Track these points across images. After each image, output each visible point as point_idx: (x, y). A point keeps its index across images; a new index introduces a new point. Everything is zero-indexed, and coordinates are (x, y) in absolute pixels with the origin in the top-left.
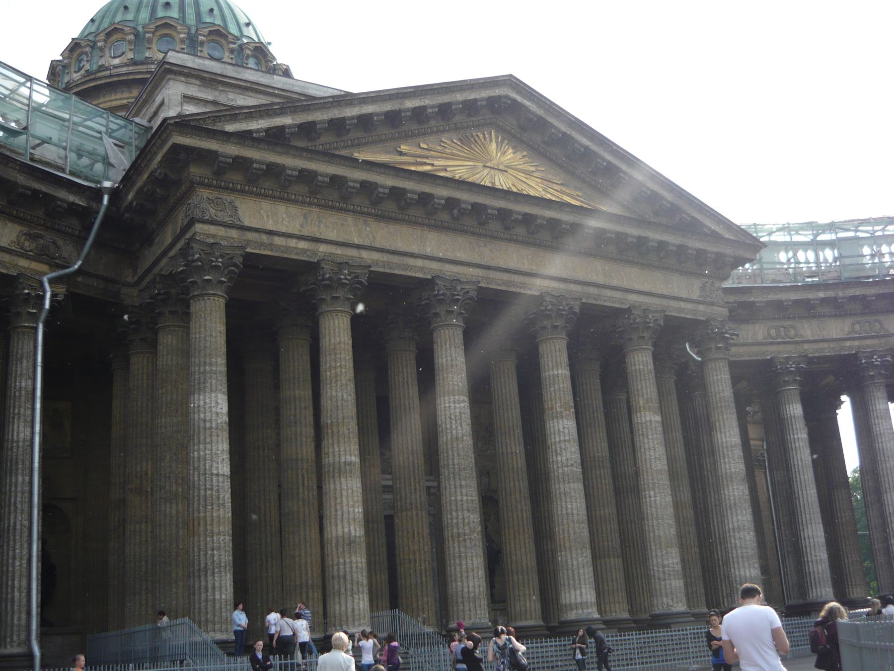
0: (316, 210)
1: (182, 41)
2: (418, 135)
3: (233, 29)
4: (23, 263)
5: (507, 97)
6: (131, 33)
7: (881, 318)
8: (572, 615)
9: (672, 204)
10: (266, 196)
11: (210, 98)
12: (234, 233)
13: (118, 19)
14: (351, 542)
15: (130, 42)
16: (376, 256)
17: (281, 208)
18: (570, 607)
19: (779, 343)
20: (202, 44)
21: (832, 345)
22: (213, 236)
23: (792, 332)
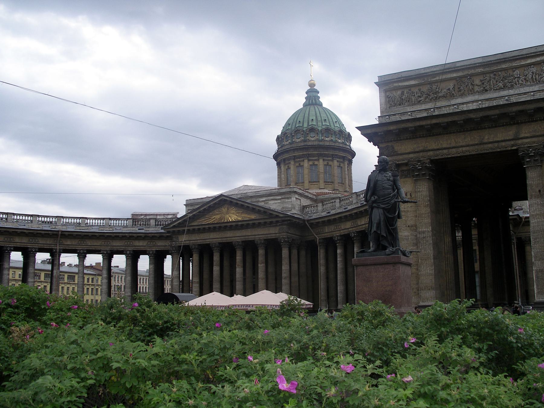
2: (209, 212)
5: (223, 199)
16: (200, 241)
20: (294, 136)
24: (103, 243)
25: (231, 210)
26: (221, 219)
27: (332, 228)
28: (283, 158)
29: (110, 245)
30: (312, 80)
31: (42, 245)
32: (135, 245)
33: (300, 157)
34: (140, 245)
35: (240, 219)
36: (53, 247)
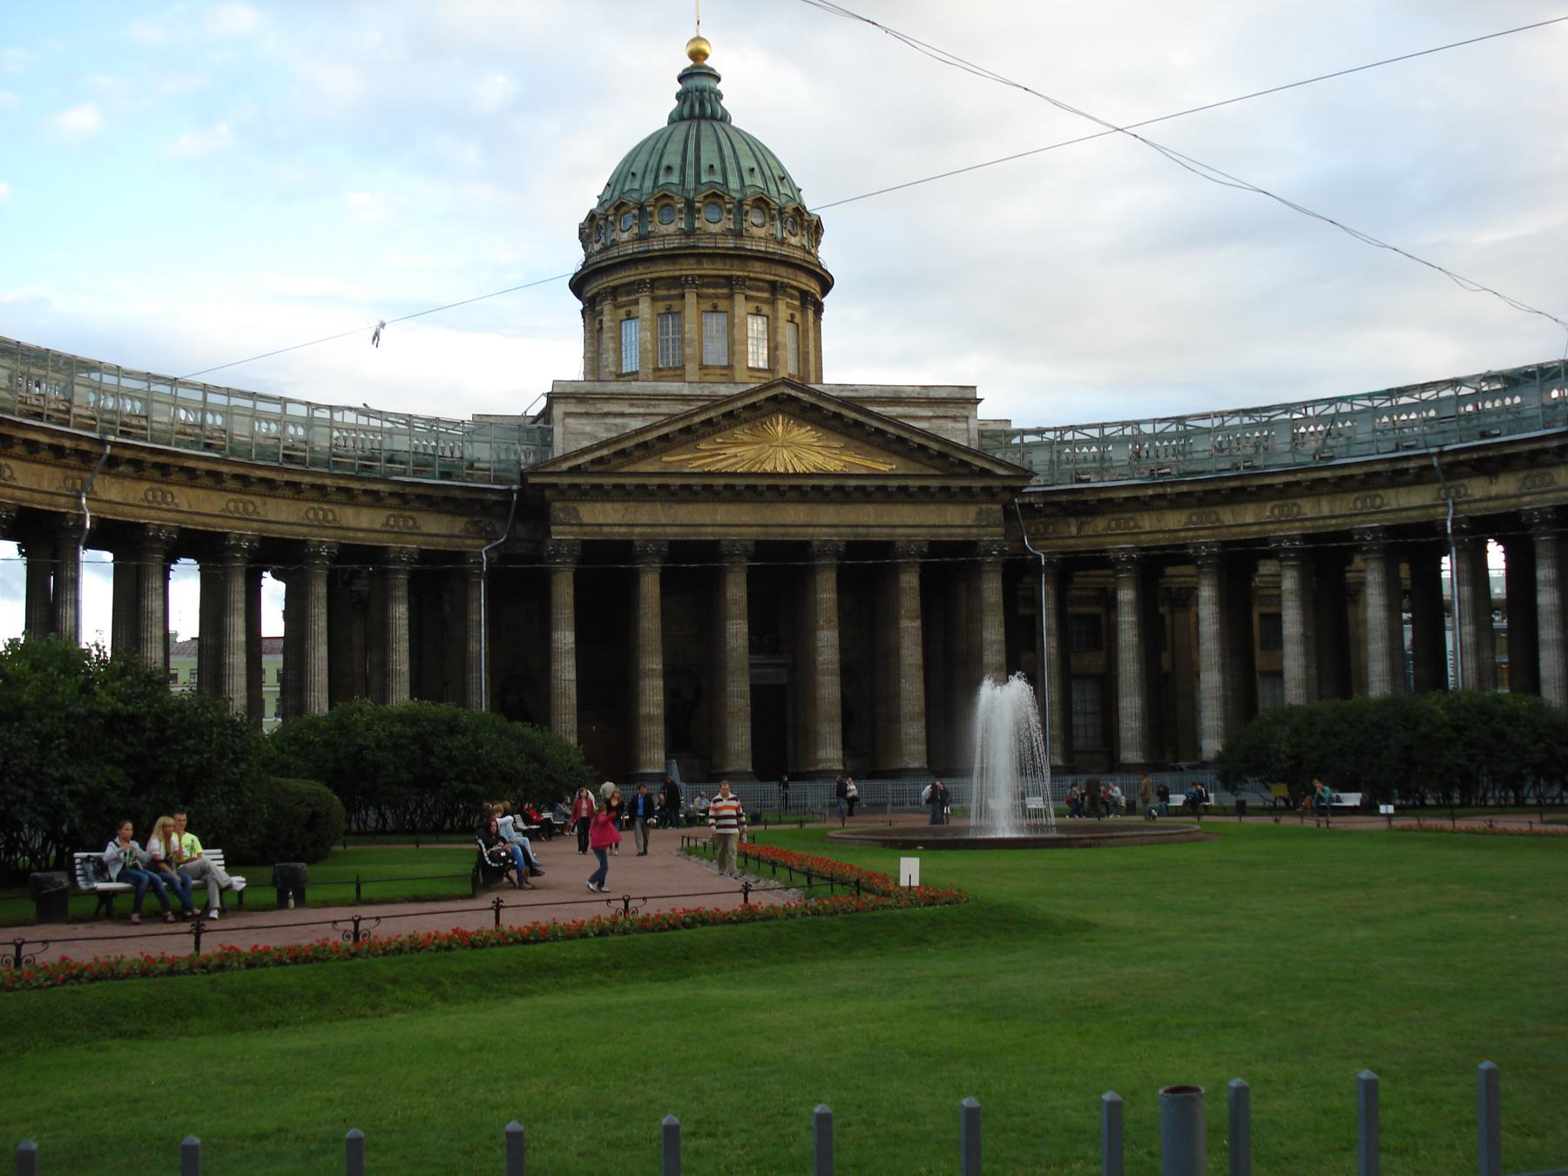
0: (632, 504)
1: (680, 211)
2: (714, 433)
3: (734, 183)
4: (469, 542)
5: (783, 394)
6: (634, 208)
7: (1218, 509)
8: (821, 766)
9: (939, 453)
10: (597, 501)
11: (583, 411)
12: (576, 529)
13: (626, 188)
14: (651, 718)
15: (634, 216)
16: (676, 530)
17: (609, 506)
18: (820, 761)
19: (1116, 535)
20: (699, 211)
21: (1167, 536)
22: (563, 533)
23: (1132, 524)
24: (232, 505)
25: (799, 435)
26: (755, 461)
27: (1100, 524)
28: (649, 276)
29: (255, 517)
30: (698, 39)
31: (26, 495)
32: (344, 523)
33: (714, 282)
34: (363, 526)
35: (834, 466)
36: (62, 505)
